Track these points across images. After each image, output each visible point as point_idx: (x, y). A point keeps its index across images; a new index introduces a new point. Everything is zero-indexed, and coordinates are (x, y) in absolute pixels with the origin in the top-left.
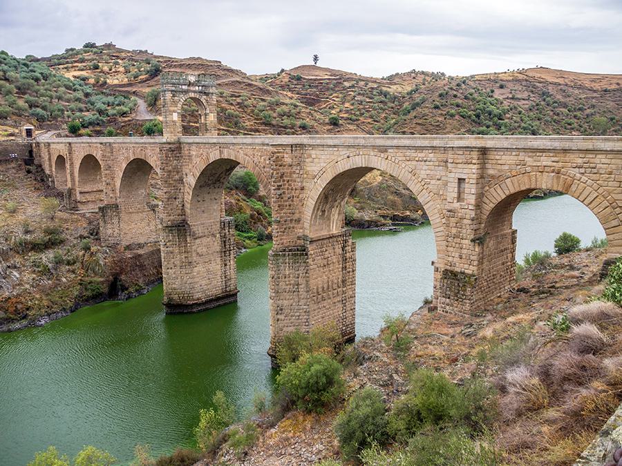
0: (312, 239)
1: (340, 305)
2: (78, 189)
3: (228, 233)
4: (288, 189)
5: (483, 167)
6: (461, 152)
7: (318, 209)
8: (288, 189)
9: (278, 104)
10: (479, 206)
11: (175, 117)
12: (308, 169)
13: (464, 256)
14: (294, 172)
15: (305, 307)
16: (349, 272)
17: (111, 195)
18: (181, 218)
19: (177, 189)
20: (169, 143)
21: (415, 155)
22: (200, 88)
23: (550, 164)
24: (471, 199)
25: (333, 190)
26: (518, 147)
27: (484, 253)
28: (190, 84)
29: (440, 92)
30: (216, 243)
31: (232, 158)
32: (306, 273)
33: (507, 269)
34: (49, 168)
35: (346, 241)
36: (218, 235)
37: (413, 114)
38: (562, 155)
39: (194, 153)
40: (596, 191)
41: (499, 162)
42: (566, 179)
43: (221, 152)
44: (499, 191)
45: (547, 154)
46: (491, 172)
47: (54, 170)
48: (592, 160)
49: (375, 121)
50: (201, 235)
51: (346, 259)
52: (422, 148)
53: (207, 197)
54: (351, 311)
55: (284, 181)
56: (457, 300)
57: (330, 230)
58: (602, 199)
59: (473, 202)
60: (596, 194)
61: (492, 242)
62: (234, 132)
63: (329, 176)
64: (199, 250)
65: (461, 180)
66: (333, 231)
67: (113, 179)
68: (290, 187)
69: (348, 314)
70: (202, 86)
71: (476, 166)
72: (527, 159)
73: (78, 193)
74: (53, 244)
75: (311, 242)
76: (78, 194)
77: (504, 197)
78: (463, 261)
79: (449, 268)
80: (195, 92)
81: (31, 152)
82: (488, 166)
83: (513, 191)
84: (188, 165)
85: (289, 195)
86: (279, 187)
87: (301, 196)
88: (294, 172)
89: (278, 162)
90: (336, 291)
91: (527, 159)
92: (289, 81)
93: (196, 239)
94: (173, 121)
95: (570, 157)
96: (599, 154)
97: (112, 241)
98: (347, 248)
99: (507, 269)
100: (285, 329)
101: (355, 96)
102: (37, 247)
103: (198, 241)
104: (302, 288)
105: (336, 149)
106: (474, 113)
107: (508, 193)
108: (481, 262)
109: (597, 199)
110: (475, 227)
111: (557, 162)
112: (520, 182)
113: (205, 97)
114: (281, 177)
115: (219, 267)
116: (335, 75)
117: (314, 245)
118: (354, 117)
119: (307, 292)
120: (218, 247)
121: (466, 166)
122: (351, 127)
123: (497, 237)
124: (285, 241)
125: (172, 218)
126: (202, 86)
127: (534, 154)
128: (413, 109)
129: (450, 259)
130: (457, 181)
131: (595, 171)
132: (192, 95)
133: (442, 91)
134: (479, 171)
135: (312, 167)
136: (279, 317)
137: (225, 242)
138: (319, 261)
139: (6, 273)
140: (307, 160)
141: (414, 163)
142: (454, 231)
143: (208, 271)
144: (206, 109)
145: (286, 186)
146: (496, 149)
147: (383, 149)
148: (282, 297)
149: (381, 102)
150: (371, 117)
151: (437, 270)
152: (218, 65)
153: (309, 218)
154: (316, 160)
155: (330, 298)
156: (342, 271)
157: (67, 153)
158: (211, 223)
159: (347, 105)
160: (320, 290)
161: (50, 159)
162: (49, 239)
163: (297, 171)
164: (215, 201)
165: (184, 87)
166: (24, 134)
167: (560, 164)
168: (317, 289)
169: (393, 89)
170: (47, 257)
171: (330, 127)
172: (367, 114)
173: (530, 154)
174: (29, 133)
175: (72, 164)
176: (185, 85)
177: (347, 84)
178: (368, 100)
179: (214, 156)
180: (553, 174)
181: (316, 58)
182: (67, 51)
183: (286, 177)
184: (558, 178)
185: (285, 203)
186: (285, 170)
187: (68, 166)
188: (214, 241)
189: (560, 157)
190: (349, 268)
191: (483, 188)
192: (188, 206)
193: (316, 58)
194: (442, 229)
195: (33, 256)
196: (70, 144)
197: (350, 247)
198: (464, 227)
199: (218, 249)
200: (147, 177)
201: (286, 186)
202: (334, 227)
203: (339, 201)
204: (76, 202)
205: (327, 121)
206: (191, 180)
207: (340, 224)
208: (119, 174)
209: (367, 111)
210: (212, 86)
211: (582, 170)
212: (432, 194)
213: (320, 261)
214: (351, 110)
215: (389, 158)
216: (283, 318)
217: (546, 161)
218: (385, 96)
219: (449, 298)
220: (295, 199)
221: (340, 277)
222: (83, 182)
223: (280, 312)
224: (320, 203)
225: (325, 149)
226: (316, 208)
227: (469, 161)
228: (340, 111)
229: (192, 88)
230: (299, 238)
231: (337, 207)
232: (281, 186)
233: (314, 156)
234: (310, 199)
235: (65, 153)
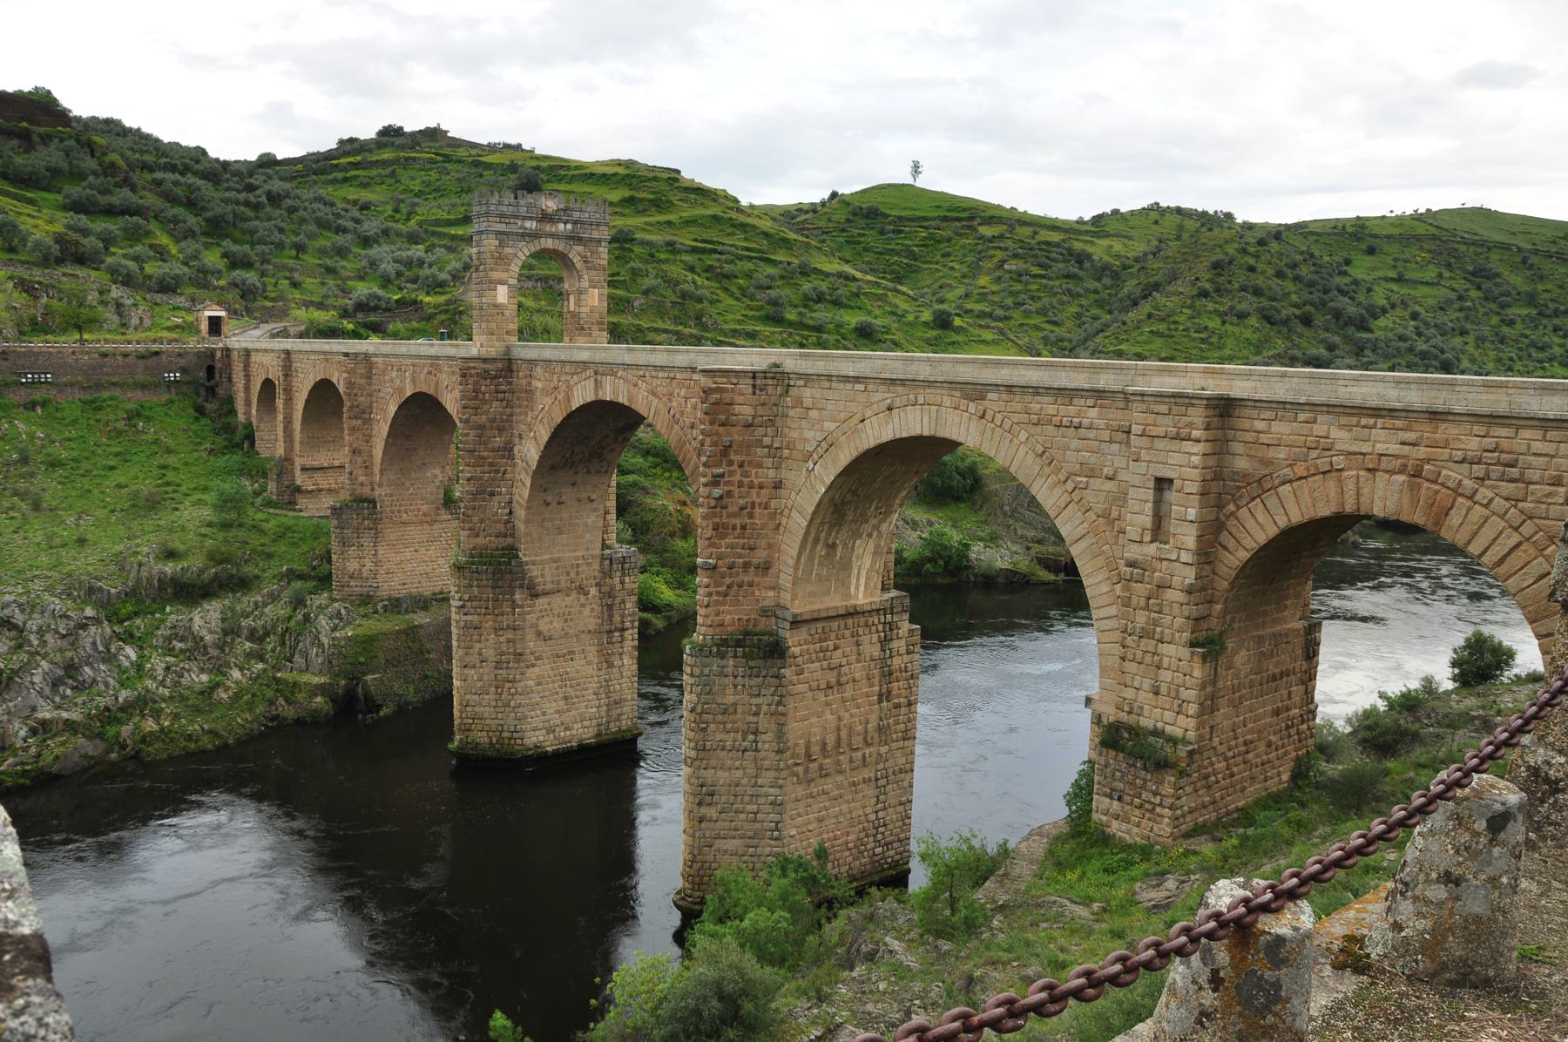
0: (796, 616)
1: (870, 791)
2: (299, 462)
3: (619, 586)
4: (740, 484)
5: (1220, 447)
6: (1163, 408)
7: (816, 540)
8: (740, 484)
9: (805, 271)
10: (1207, 554)
11: (502, 295)
12: (795, 434)
13: (1164, 690)
14: (759, 443)
15: (772, 790)
16: (898, 706)
17: (362, 478)
18: (502, 542)
19: (497, 472)
20: (485, 360)
21: (1051, 409)
22: (569, 226)
23: (1394, 448)
24: (1188, 537)
25: (854, 493)
26: (1314, 399)
27: (1220, 684)
28: (545, 217)
29: (1214, 258)
30: (587, 612)
31: (623, 400)
32: (779, 703)
33: (1288, 727)
34: (246, 409)
35: (891, 626)
36: (593, 591)
37: (1146, 308)
38: (1426, 427)
39: (540, 385)
40: (1516, 529)
41: (1264, 438)
42: (1437, 492)
43: (598, 385)
44: (1261, 517)
45: (1389, 422)
46: (1242, 464)
47: (254, 412)
48: (1505, 444)
49: (1048, 322)
50: (549, 587)
51: (891, 674)
52: (1066, 394)
53: (568, 494)
54: (901, 809)
55: (731, 463)
56: (1140, 807)
57: (848, 596)
58: (1533, 552)
59: (1190, 541)
60: (1515, 539)
61: (1243, 653)
62: (692, 336)
63: (845, 457)
64: (544, 626)
65: (1162, 484)
67: (368, 439)
68: (746, 480)
69: (892, 815)
70: (575, 223)
71: (1202, 444)
72: (1336, 433)
73: (299, 468)
74: (221, 587)
75: (796, 623)
76: (298, 473)
77: (1273, 531)
78: (1162, 700)
79: (1124, 717)
80: (553, 236)
81: (210, 370)
82: (1238, 448)
83: (1296, 518)
84: (526, 414)
85: (742, 502)
86: (716, 481)
87: (773, 504)
88: (759, 443)
89: (717, 407)
90: (859, 754)
91: (1336, 433)
92: (848, 221)
93: (536, 596)
94: (496, 306)
95: (1447, 430)
96: (1523, 427)
97: (356, 587)
98: (895, 644)
99: (1288, 727)
100: (718, 844)
101: (1004, 261)
102: (189, 592)
103: (541, 602)
104: (767, 740)
105: (861, 387)
106: (1298, 312)
107: (1283, 522)
108: (1208, 706)
109: (1519, 552)
110: (1194, 611)
111: (1414, 445)
112: (1316, 494)
113: (580, 248)
114: (725, 452)
115: (590, 670)
116: (957, 209)
117: (803, 633)
118: (999, 312)
119: (779, 752)
120: (593, 621)
121: (1174, 445)
122: (988, 335)
123: (1260, 640)
124: (728, 617)
125: (481, 541)
126: (575, 223)
127: (1354, 420)
128: (1145, 297)
129: (1129, 693)
130: (1152, 484)
131: (1514, 472)
132: (549, 243)
133: (1220, 257)
134: (1211, 461)
135: (804, 433)
136: (704, 810)
137: (610, 607)
138: (814, 671)
139: (108, 650)
140: (792, 413)
141: (1050, 429)
142: (1141, 618)
143: (564, 678)
144: (580, 277)
145: (737, 477)
146: (1257, 403)
147: (975, 392)
148: (713, 762)
149: (1068, 277)
150: (1042, 312)
151: (1097, 719)
152: (673, 176)
153: (791, 562)
154: (814, 414)
155: (841, 772)
156: (880, 701)
157: (281, 374)
158: (577, 558)
159: (983, 280)
160: (815, 749)
161: (247, 388)
162: (216, 573)
163: (767, 441)
164: (589, 506)
165: (528, 224)
166: (204, 326)
167: (1422, 452)
168: (808, 746)
169: (1099, 250)
170: (206, 619)
171: (934, 333)
172: (1032, 306)
173: (1344, 420)
174: (215, 324)
175: (289, 401)
176: (531, 219)
177: (987, 231)
178: (1036, 270)
179: (583, 394)
180: (1401, 478)
181: (916, 168)
182: (341, 142)
183: (737, 453)
184: (1413, 488)
185: (733, 521)
186: (737, 435)
187: (280, 403)
188: (583, 606)
189: (1425, 430)
190: (899, 696)
191: (1220, 506)
192: (520, 513)
193: (916, 168)
194: (1113, 611)
195: (174, 615)
196: (288, 353)
197: (902, 643)
198: (1166, 610)
199: (593, 623)
200: (446, 437)
201: (737, 477)
202: (862, 588)
203: (873, 521)
204: (298, 490)
205: (927, 316)
206: (530, 451)
207: (877, 580)
208: (382, 429)
209: (1032, 298)
210: (598, 224)
211: (1478, 470)
212: (1091, 516)
213: (818, 675)
214: (993, 293)
215: (989, 416)
216: (715, 816)
217: (1384, 441)
218: (1080, 262)
219: (1120, 799)
220: (757, 511)
221: (873, 718)
222: (312, 443)
223: (708, 799)
224: (822, 524)
225: (834, 385)
226: (811, 537)
227: (1184, 432)
228: (967, 295)
229: (548, 228)
230: (765, 612)
231: (870, 536)
232: (722, 476)
233: (808, 402)
234: (794, 514)
235: (275, 374)
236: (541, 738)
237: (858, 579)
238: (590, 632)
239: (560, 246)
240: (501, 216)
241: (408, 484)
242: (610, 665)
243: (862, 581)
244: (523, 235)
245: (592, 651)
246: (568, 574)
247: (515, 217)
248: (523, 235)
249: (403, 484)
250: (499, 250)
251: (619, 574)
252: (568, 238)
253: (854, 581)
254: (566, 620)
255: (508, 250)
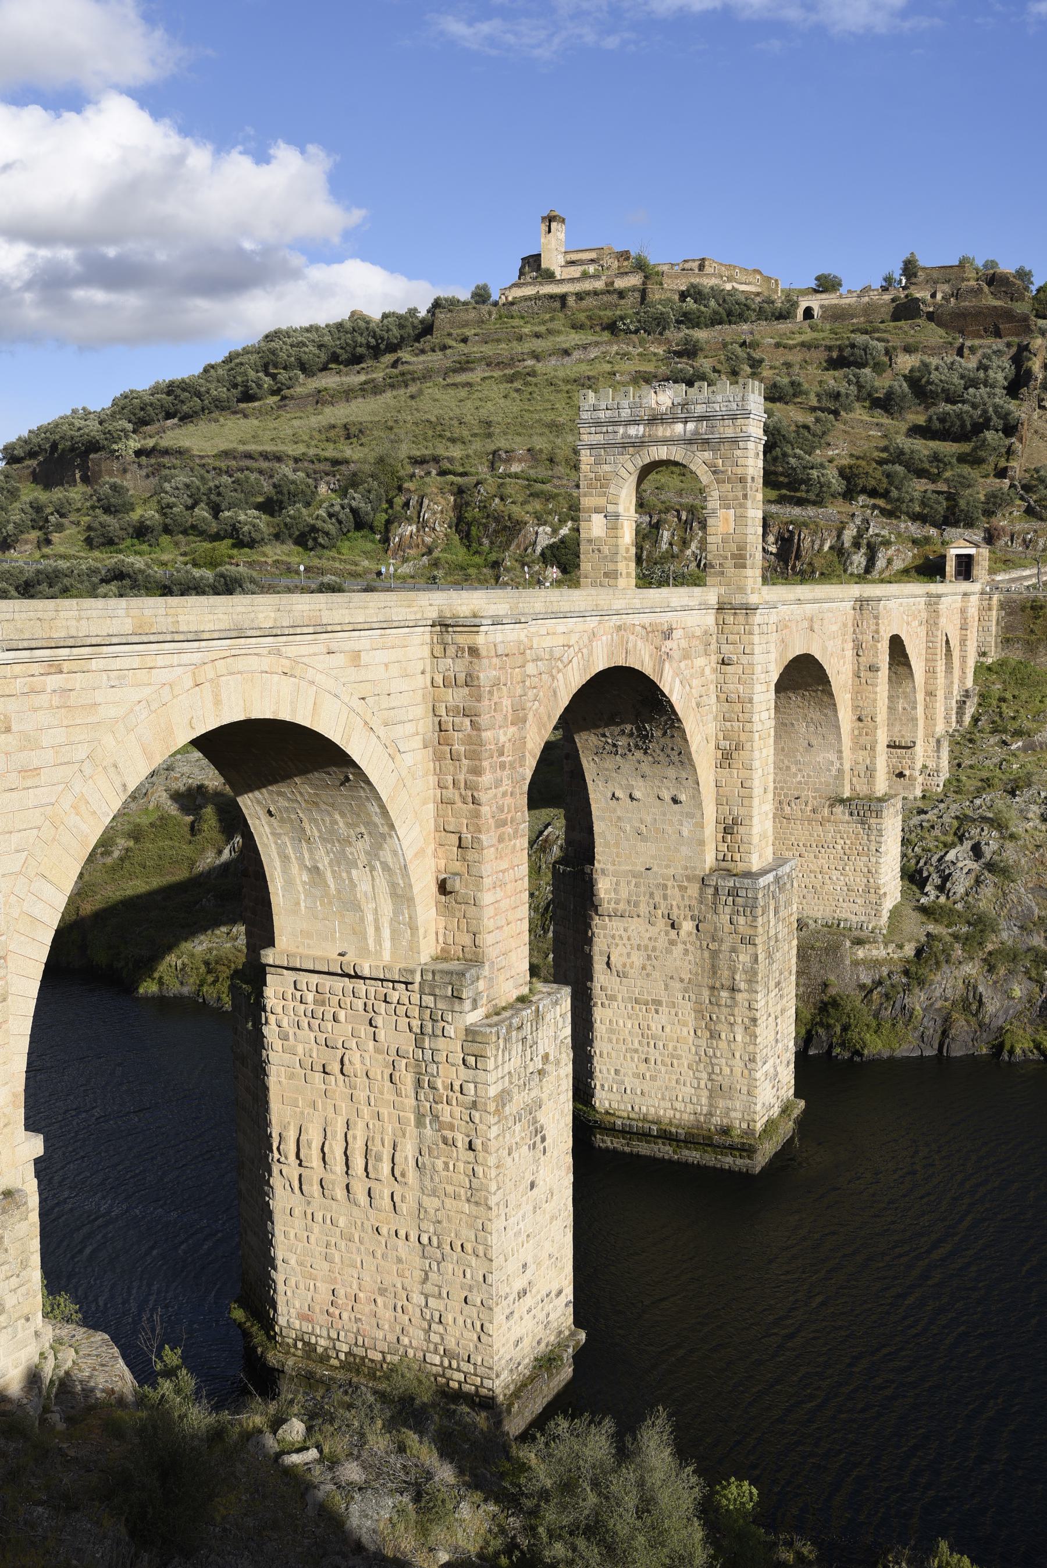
3: (728, 927)
28: (655, 419)
36: (688, 926)
66: (379, 953)
70: (702, 418)
113: (708, 455)
132: (662, 453)
137: (715, 954)
165: (632, 431)
176: (636, 422)
188: (672, 943)
229: (661, 431)
236: (615, 1105)
237: (377, 929)
238: (682, 980)
239: (677, 454)
240: (598, 424)
241: (794, 769)
242: (714, 1035)
243: (386, 933)
244: (624, 446)
245: (687, 1010)
246: (652, 895)
247: (615, 423)
248: (624, 446)
249: (788, 768)
250: (596, 468)
251: (728, 910)
252: (690, 442)
253: (371, 931)
254: (649, 957)
255: (607, 468)
